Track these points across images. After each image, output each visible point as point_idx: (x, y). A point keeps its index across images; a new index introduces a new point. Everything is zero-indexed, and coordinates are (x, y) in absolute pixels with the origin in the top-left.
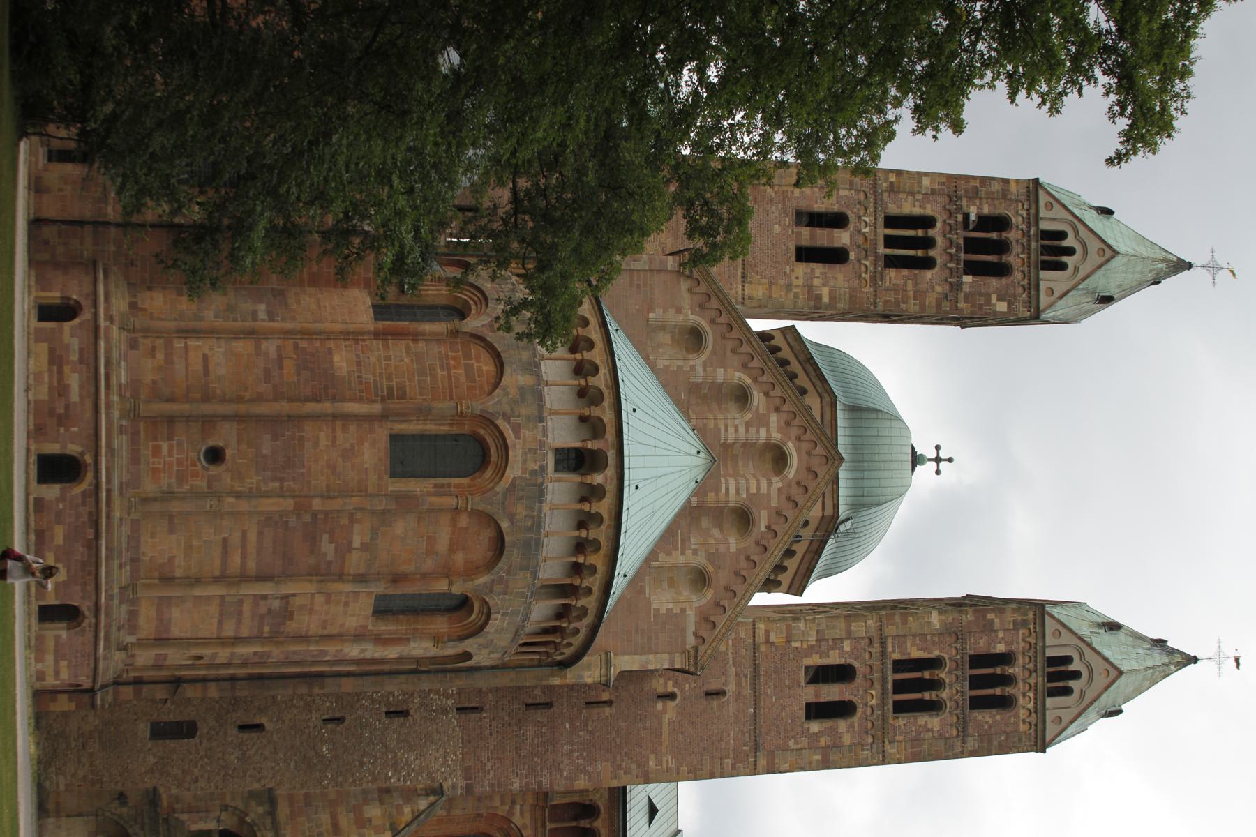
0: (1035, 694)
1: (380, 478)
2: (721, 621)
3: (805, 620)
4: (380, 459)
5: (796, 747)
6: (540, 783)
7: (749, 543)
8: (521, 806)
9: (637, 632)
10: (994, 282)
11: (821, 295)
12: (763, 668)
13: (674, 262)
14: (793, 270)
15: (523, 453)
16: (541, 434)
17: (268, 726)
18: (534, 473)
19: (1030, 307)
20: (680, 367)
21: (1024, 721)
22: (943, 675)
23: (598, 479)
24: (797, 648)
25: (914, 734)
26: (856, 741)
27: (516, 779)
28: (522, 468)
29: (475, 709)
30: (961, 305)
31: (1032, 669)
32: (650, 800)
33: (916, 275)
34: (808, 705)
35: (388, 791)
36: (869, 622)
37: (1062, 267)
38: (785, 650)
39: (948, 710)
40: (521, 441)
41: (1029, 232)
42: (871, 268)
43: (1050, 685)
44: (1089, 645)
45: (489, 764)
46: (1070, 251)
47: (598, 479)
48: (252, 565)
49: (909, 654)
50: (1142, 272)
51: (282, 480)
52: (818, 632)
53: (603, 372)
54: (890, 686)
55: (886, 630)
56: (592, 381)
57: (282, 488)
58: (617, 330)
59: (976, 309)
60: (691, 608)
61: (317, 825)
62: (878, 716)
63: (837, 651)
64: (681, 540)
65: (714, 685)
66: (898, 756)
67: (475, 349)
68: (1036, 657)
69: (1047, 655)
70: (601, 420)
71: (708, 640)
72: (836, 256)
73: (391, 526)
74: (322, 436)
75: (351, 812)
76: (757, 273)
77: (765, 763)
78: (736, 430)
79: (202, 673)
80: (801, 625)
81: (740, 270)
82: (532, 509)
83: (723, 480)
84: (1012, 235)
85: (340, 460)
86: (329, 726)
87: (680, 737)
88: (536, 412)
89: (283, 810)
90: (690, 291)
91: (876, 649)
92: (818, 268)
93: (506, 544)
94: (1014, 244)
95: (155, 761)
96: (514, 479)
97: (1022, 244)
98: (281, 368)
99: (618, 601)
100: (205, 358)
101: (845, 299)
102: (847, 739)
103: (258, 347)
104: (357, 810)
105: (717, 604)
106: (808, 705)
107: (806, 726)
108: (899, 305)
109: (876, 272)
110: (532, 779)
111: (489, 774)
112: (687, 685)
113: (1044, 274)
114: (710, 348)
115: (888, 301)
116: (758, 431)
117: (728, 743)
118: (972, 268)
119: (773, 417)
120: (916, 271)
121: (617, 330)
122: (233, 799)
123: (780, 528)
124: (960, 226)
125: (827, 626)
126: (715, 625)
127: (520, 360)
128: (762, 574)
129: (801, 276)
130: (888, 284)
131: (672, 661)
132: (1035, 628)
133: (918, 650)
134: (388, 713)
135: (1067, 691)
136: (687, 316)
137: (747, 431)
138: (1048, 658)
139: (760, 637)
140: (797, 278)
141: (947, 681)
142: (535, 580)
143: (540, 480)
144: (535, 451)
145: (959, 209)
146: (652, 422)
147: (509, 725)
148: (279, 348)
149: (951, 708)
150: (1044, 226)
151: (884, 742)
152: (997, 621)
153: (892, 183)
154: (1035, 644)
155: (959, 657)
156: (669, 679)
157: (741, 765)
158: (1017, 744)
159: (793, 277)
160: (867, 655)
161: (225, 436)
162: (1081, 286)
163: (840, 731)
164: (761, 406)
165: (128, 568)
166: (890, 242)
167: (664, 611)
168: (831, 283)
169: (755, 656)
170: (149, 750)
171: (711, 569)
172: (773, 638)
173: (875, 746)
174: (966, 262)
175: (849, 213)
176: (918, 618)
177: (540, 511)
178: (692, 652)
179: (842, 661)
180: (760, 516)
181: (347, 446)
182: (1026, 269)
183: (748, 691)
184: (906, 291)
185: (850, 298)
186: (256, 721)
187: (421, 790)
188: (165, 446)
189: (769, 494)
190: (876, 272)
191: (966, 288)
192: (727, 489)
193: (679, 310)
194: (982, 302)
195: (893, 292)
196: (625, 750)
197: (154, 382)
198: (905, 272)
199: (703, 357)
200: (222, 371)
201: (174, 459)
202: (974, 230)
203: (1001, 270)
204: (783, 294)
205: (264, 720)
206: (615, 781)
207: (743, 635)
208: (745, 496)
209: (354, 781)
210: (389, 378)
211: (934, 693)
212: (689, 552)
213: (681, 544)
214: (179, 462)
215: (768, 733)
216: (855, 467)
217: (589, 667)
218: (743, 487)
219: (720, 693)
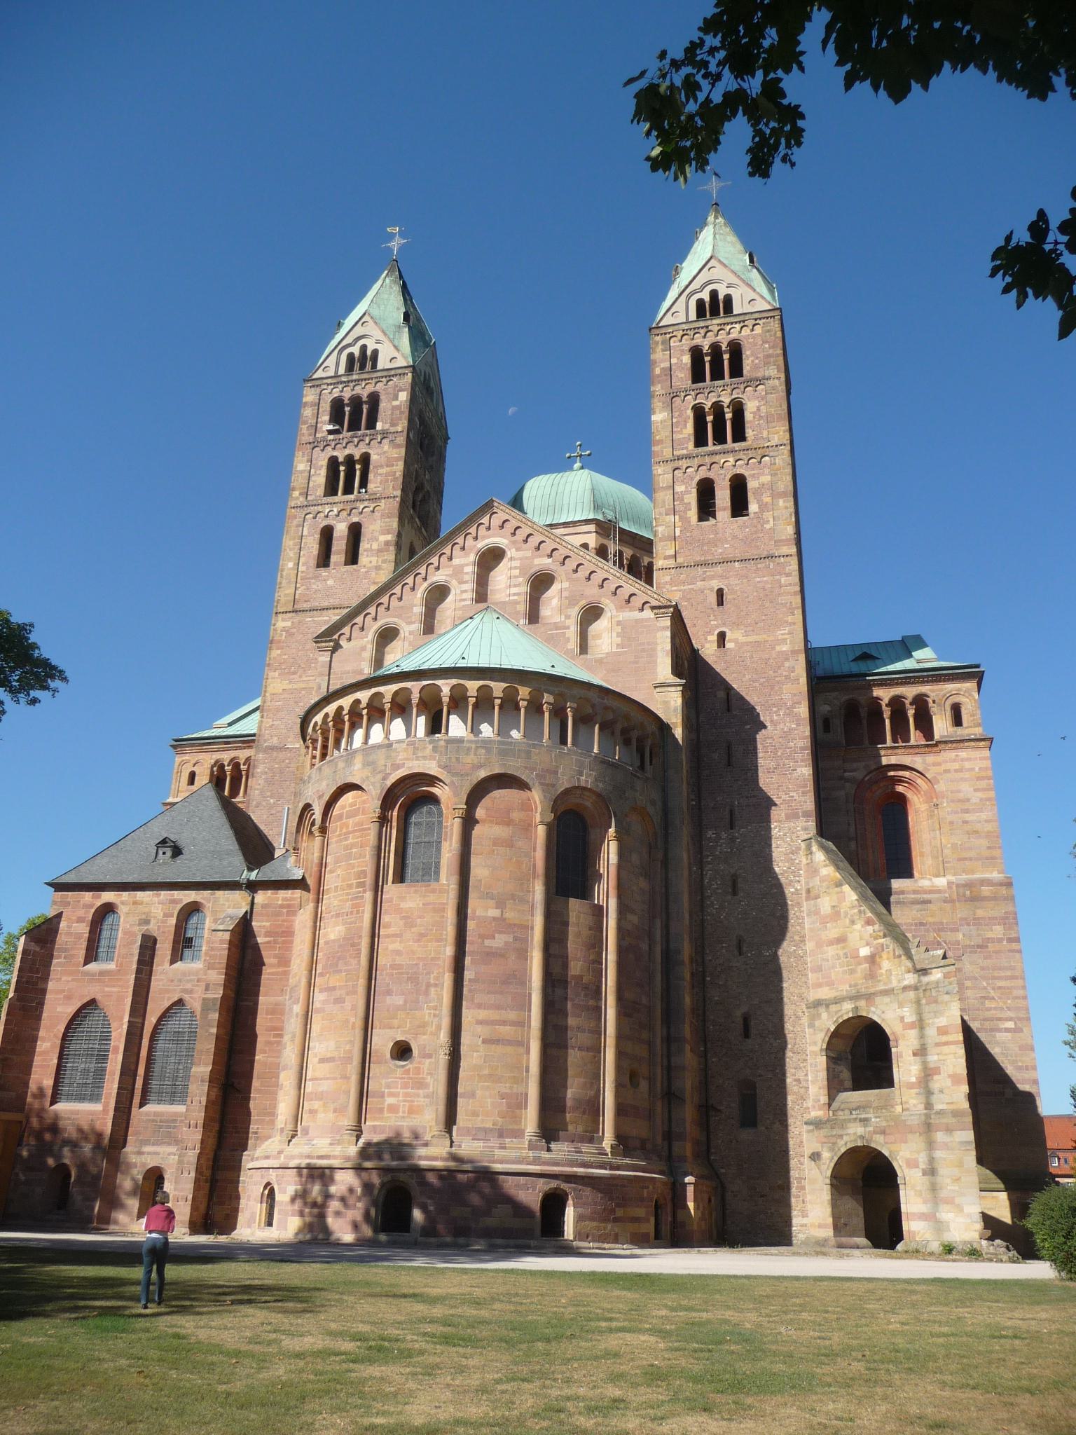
0: (728, 324)
1: (433, 891)
4: (416, 892)
5: (771, 522)
6: (802, 749)
7: (561, 573)
8: (845, 771)
9: (637, 663)
10: (383, 405)
12: (698, 558)
15: (416, 760)
16: (401, 744)
17: (744, 1009)
18: (435, 749)
19: (404, 374)
21: (752, 330)
22: (709, 404)
23: (446, 691)
25: (762, 422)
26: (766, 471)
27: (799, 770)
29: (731, 813)
30: (399, 429)
31: (705, 330)
32: (855, 660)
34: (733, 516)
35: (808, 891)
36: (660, 471)
37: (375, 353)
39: (740, 396)
41: (345, 382)
42: (366, 503)
43: (722, 315)
44: (687, 287)
45: (783, 797)
46: (364, 348)
47: (446, 691)
48: (512, 1015)
49: (689, 435)
50: (390, 294)
51: (429, 985)
52: (667, 515)
54: (718, 447)
57: (436, 985)
59: (403, 416)
61: (838, 959)
62: (744, 454)
63: (685, 496)
65: (713, 598)
66: (781, 433)
67: (337, 810)
68: (694, 329)
69: (695, 319)
70: (396, 693)
72: (355, 532)
73: (480, 881)
74: (391, 947)
75: (826, 927)
77: (786, 547)
78: (465, 591)
79: (659, 1071)
80: (660, 529)
82: (469, 749)
84: (347, 394)
85: (413, 930)
86: (745, 949)
87: (761, 625)
89: (825, 993)
90: (349, 639)
91: (684, 463)
92: (364, 545)
93: (502, 771)
94: (354, 393)
95: (778, 1123)
96: (439, 766)
97: (354, 386)
98: (334, 988)
100: (322, 1061)
102: (766, 479)
103: (319, 1011)
104: (824, 921)
105: (615, 593)
106: (733, 516)
107: (751, 515)
110: (799, 756)
111: (793, 797)
112: (712, 623)
113: (380, 366)
114: (396, 620)
115: (393, 487)
116: (467, 573)
117: (767, 582)
118: (371, 425)
119: (456, 561)
120: (371, 467)
122: (815, 1043)
124: (337, 436)
126: (634, 594)
127: (344, 768)
129: (369, 559)
131: (664, 628)
132: (669, 333)
133: (685, 425)
134: (735, 893)
135: (728, 300)
136: (368, 642)
137: (466, 582)
138: (697, 318)
139: (671, 563)
140: (371, 562)
141: (714, 400)
143: (442, 743)
145: (324, 439)
147: (746, 779)
148: (321, 991)
149: (738, 394)
150: (342, 370)
151: (768, 447)
152: (662, 365)
153: (300, 494)
154: (683, 330)
155: (693, 393)
156: (706, 639)
157: (787, 568)
158: (773, 333)
159: (370, 565)
161: (383, 1041)
162: (391, 337)
163: (757, 485)
164: (446, 573)
165: (507, 1140)
166: (348, 490)
167: (619, 640)
170: (767, 1128)
171: (583, 602)
173: (771, 454)
174: (368, 428)
175: (322, 526)
178: (655, 611)
179: (695, 491)
181: (402, 923)
182: (374, 381)
183: (719, 569)
185: (389, 517)
186: (739, 1020)
187: (807, 859)
188: (390, 1101)
189: (521, 559)
191: (387, 426)
192: (514, 594)
193: (363, 649)
194: (398, 412)
196: (771, 673)
197: (335, 1111)
198: (371, 476)
200: (332, 1044)
201: (402, 1091)
202: (342, 426)
203: (374, 399)
204: (382, 572)
205: (738, 1013)
206: (801, 680)
207: (668, 578)
208: (521, 579)
209: (799, 924)
210: (350, 886)
211: (726, 410)
212: (568, 622)
214: (405, 1086)
215: (758, 547)
217: (666, 703)
218: (514, 581)
219: (720, 593)
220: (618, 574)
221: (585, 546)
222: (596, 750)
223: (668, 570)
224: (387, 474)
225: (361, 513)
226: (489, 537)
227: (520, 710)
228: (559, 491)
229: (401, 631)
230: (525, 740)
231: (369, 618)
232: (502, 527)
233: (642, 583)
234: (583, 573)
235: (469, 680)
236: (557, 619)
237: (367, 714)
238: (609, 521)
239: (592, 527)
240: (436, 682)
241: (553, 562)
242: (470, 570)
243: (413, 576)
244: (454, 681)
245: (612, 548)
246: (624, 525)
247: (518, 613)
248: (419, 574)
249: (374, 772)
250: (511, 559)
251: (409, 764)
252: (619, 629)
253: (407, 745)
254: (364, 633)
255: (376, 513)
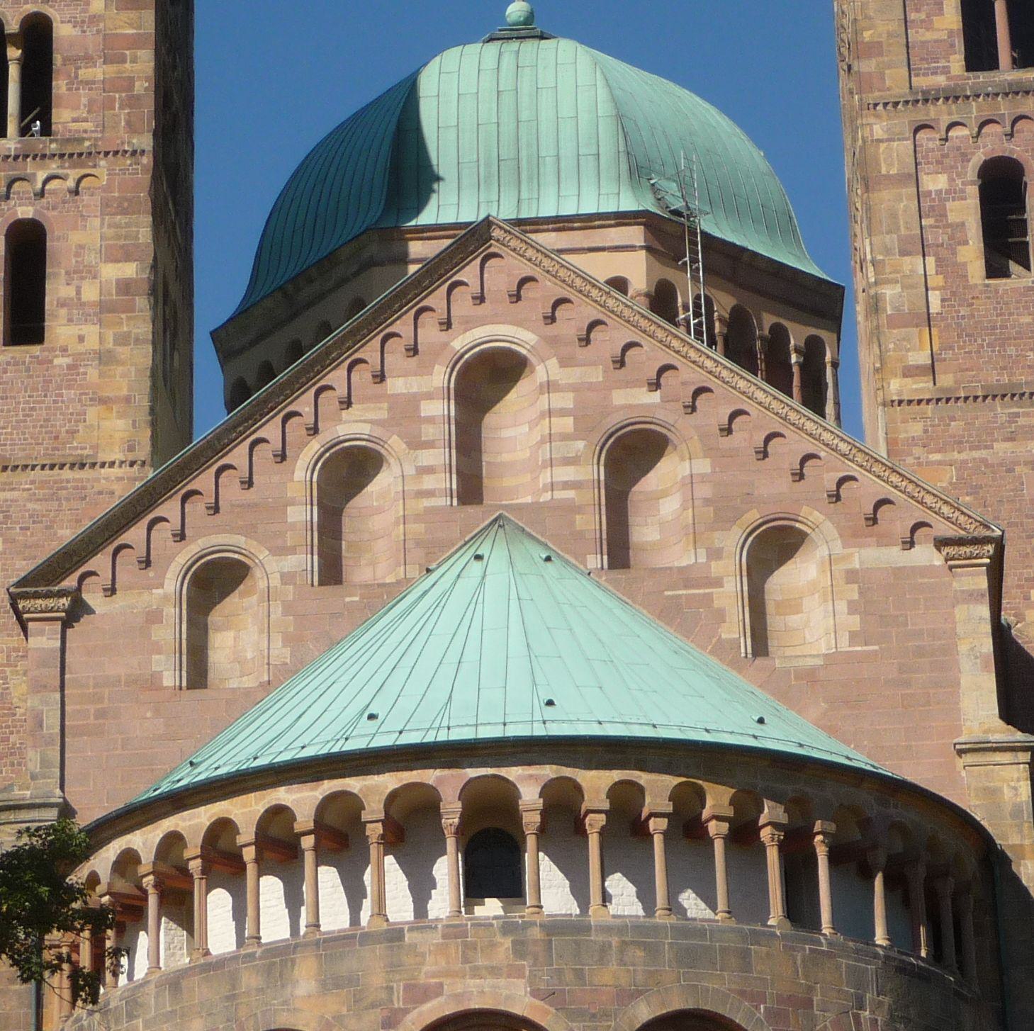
2: (869, 487)
3: (876, 283)
11: (118, 281)
12: (995, 378)
13: (41, 633)
14: (64, 350)
15: (473, 977)
18: (520, 949)
20: (288, 609)
23: (530, 796)
24: (943, 300)
28: (509, 976)
33: (66, 60)
36: (878, 130)
38: (948, 326)
40: (446, 982)
42: (54, 167)
47: (530, 796)
49: (951, 34)
52: (904, 253)
53: (283, 795)
55: (896, 91)
56: (304, 818)
58: (192, 764)
60: (844, 558)
63: (949, 205)
64: (686, 587)
70: (393, 797)
71: (920, 514)
76: (72, 433)
78: (430, 470)
80: (889, 292)
81: (67, 474)
82: (604, 949)
83: (547, 496)
88: (379, 949)
90: (111, 591)
91: (941, 113)
92: (57, 290)
93: (690, 1005)
96: (535, 993)
99: (832, 731)
101: (128, 225)
108: (138, 97)
109: (62, 156)
114: (240, 540)
115: (128, 123)
116: (431, 420)
119: (396, 385)
120: (58, 59)
121: (192, 764)
123: (649, 357)
125: (889, 232)
127: (260, 990)
128: (760, 395)
129: (73, 330)
130: (88, 126)
131: (971, 596)
133: (940, 11)
136: (166, 597)
137: (430, 445)
139: (921, 387)
140: (81, 339)
142: (774, 934)
143: (536, 933)
144: (469, 948)
146: (401, 674)
159: (80, 348)
160: (956, 133)
167: (855, 622)
168: (91, 258)
169: (966, 398)
172: (921, 357)
176: (867, 17)
177: (607, 929)
178: (946, 550)
179: (973, 192)
180: (630, 407)
184: (103, 82)
185: (124, 212)
189: (575, 388)
190: (62, 156)
192: (566, 485)
193: (154, 617)
195: (108, 113)
198: (60, 86)
199: (263, 555)
204: (120, 369)
207: (916, 429)
208: (580, 444)
212: (716, 568)
213: (693, 587)
216: (530, 179)
217: (991, 793)
218: (561, 449)
220: (843, 447)
221: (619, 284)
222: (880, 938)
223: (915, 407)
224: (109, 85)
225: (41, 194)
226: (483, 322)
227: (710, 843)
228: (524, 115)
229: (257, 573)
230: (732, 923)
231: (162, 534)
232: (517, 297)
233: (758, 381)
234: (746, 437)
235: (588, 767)
236: (683, 557)
237: (316, 848)
238: (677, 213)
239: (635, 234)
240: (503, 772)
241: (665, 400)
242: (439, 409)
243: (279, 418)
244: (549, 771)
245: (688, 291)
246: (712, 225)
247: (579, 536)
248: (296, 414)
249: (358, 1003)
250: (549, 387)
251: (452, 986)
252: (853, 593)
253: (444, 937)
254: (151, 573)
255: (85, 197)
